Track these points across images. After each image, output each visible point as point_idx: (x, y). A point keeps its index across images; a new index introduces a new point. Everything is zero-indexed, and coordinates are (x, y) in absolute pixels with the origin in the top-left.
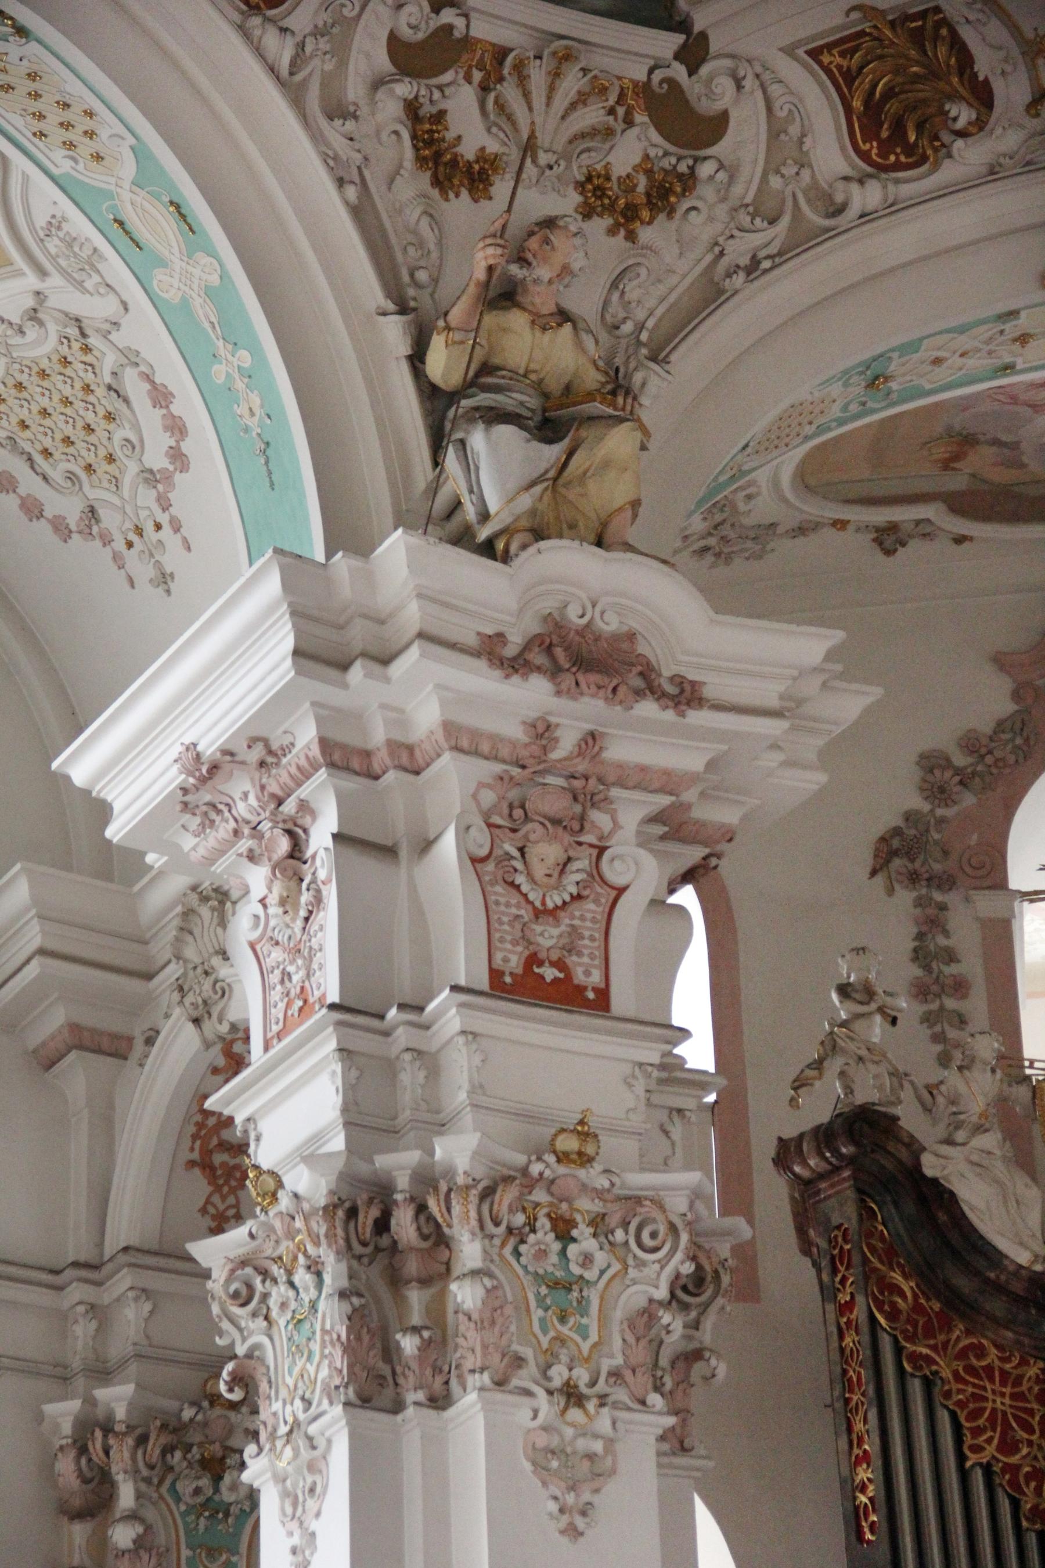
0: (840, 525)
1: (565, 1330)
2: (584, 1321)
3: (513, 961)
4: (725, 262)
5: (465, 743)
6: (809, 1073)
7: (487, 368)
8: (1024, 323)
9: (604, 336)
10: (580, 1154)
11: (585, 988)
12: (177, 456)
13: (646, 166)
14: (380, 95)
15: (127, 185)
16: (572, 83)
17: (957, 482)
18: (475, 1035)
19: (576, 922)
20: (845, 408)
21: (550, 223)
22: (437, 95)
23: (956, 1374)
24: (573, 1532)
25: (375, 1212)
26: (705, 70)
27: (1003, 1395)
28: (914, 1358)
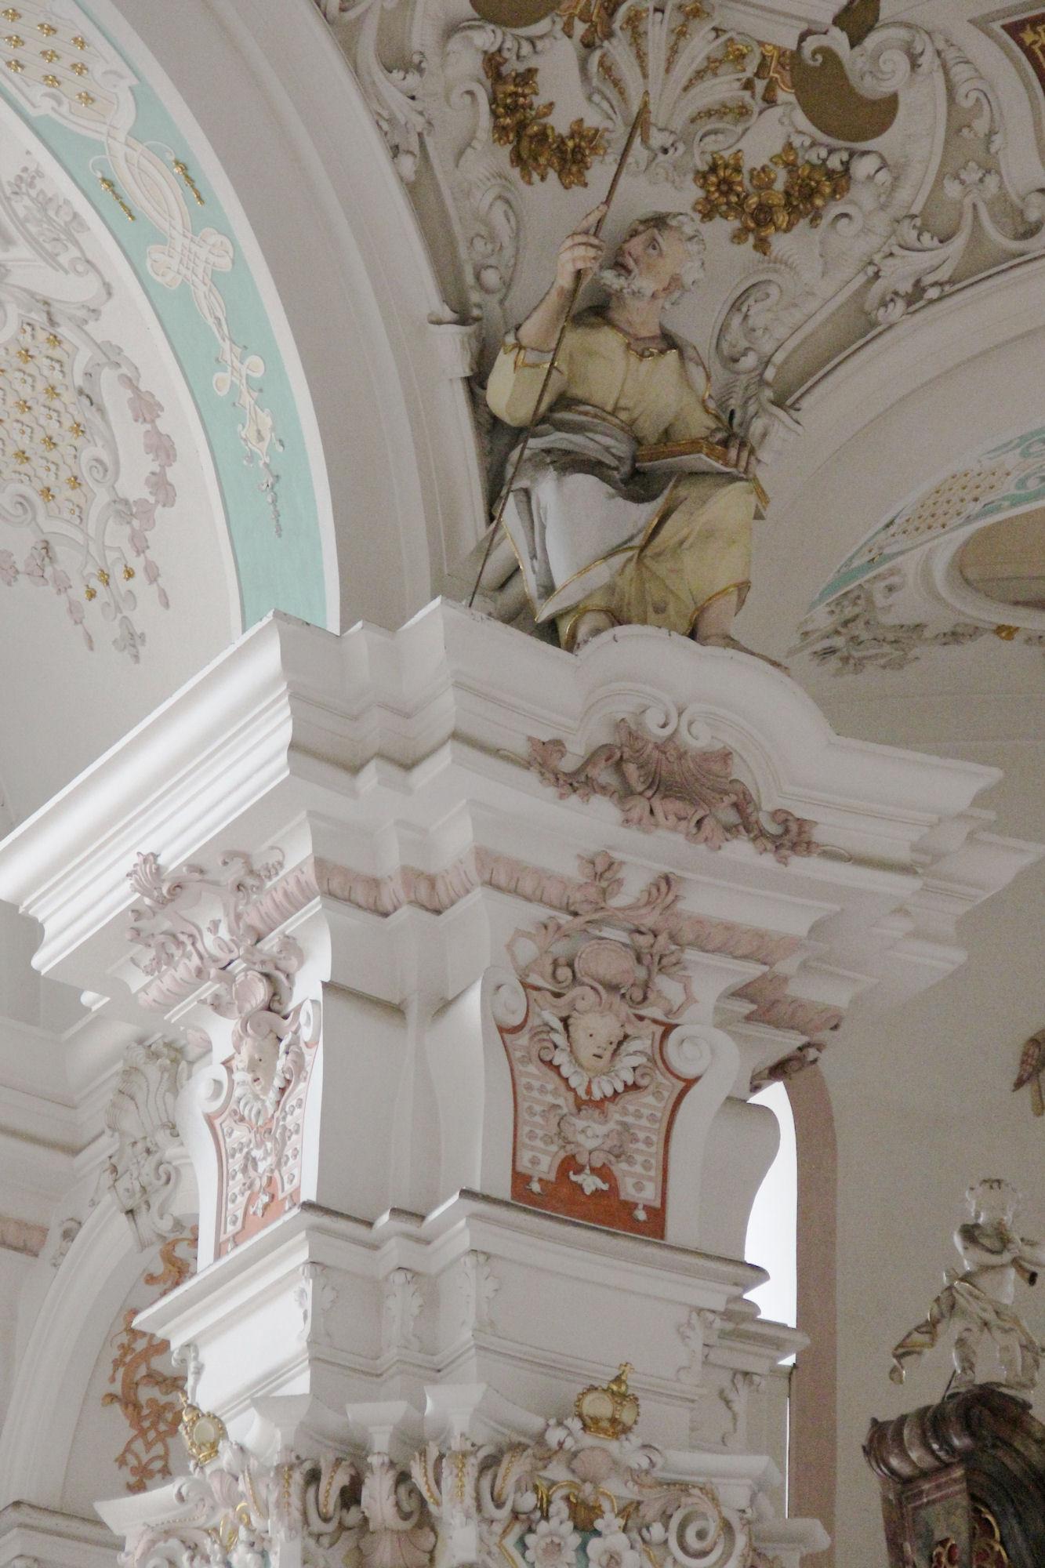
0: (1005, 632)
3: (543, 1164)
4: (878, 288)
5: (502, 879)
6: (918, 1338)
7: (564, 401)
9: (716, 368)
10: (614, 1421)
11: (636, 1205)
12: (161, 486)
13: (788, 157)
14: (455, 44)
15: (122, 136)
16: (700, 45)
18: (488, 1256)
19: (630, 1120)
20: (1022, 483)
21: (659, 221)
22: (526, 48)
25: (342, 1479)
26: (871, 41)
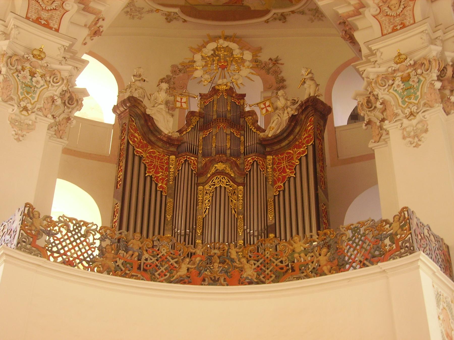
0: (158, 10)
1: (28, 96)
2: (34, 95)
3: (34, 17)
10: (39, 55)
18: (17, 27)
23: (147, 157)
24: (18, 140)
27: (158, 162)
28: (137, 151)
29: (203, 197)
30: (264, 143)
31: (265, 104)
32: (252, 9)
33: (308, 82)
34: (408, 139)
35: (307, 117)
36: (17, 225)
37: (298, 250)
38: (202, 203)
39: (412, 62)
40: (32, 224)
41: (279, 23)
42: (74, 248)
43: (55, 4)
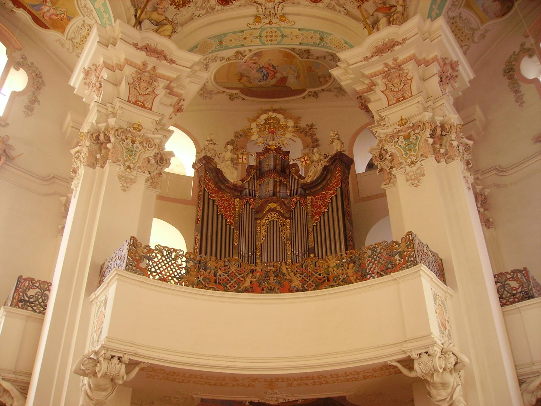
3: (134, 100)
8: (245, 34)
17: (241, 86)
25: (97, 134)
28: (211, 196)
29: (260, 229)
30: (304, 187)
31: (304, 159)
32: (293, 89)
33: (336, 141)
34: (411, 181)
35: (335, 167)
36: (125, 252)
37: (331, 266)
38: (260, 233)
39: (411, 125)
40: (136, 251)
41: (313, 99)
42: (167, 268)
43: (148, 90)
